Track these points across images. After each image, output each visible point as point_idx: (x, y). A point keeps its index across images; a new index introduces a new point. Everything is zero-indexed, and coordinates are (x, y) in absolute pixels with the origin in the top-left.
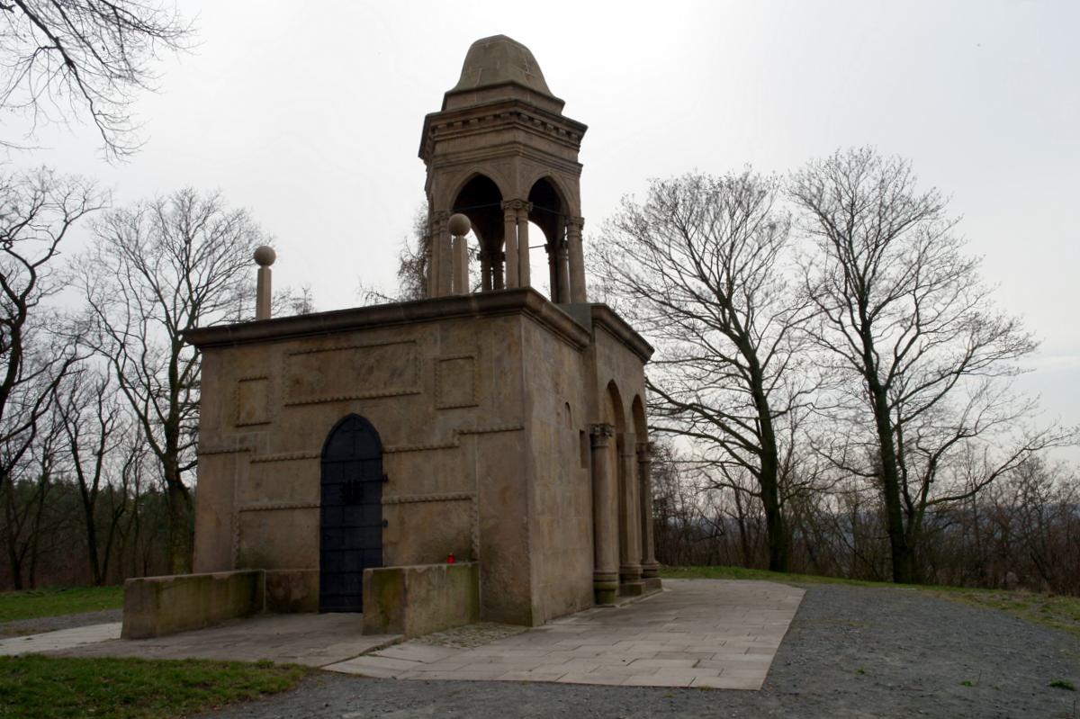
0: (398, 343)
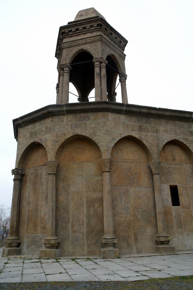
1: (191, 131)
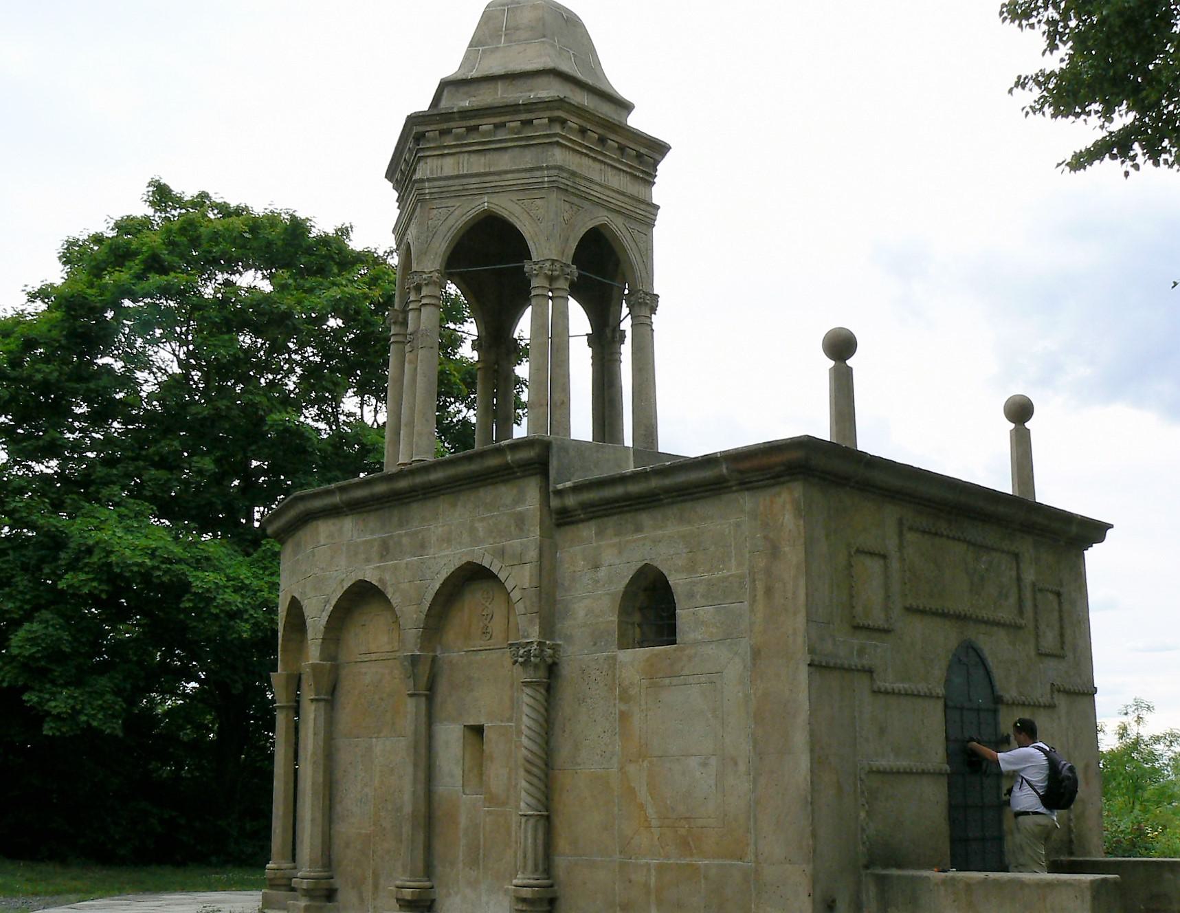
0: (1003, 552)
1: (520, 513)
